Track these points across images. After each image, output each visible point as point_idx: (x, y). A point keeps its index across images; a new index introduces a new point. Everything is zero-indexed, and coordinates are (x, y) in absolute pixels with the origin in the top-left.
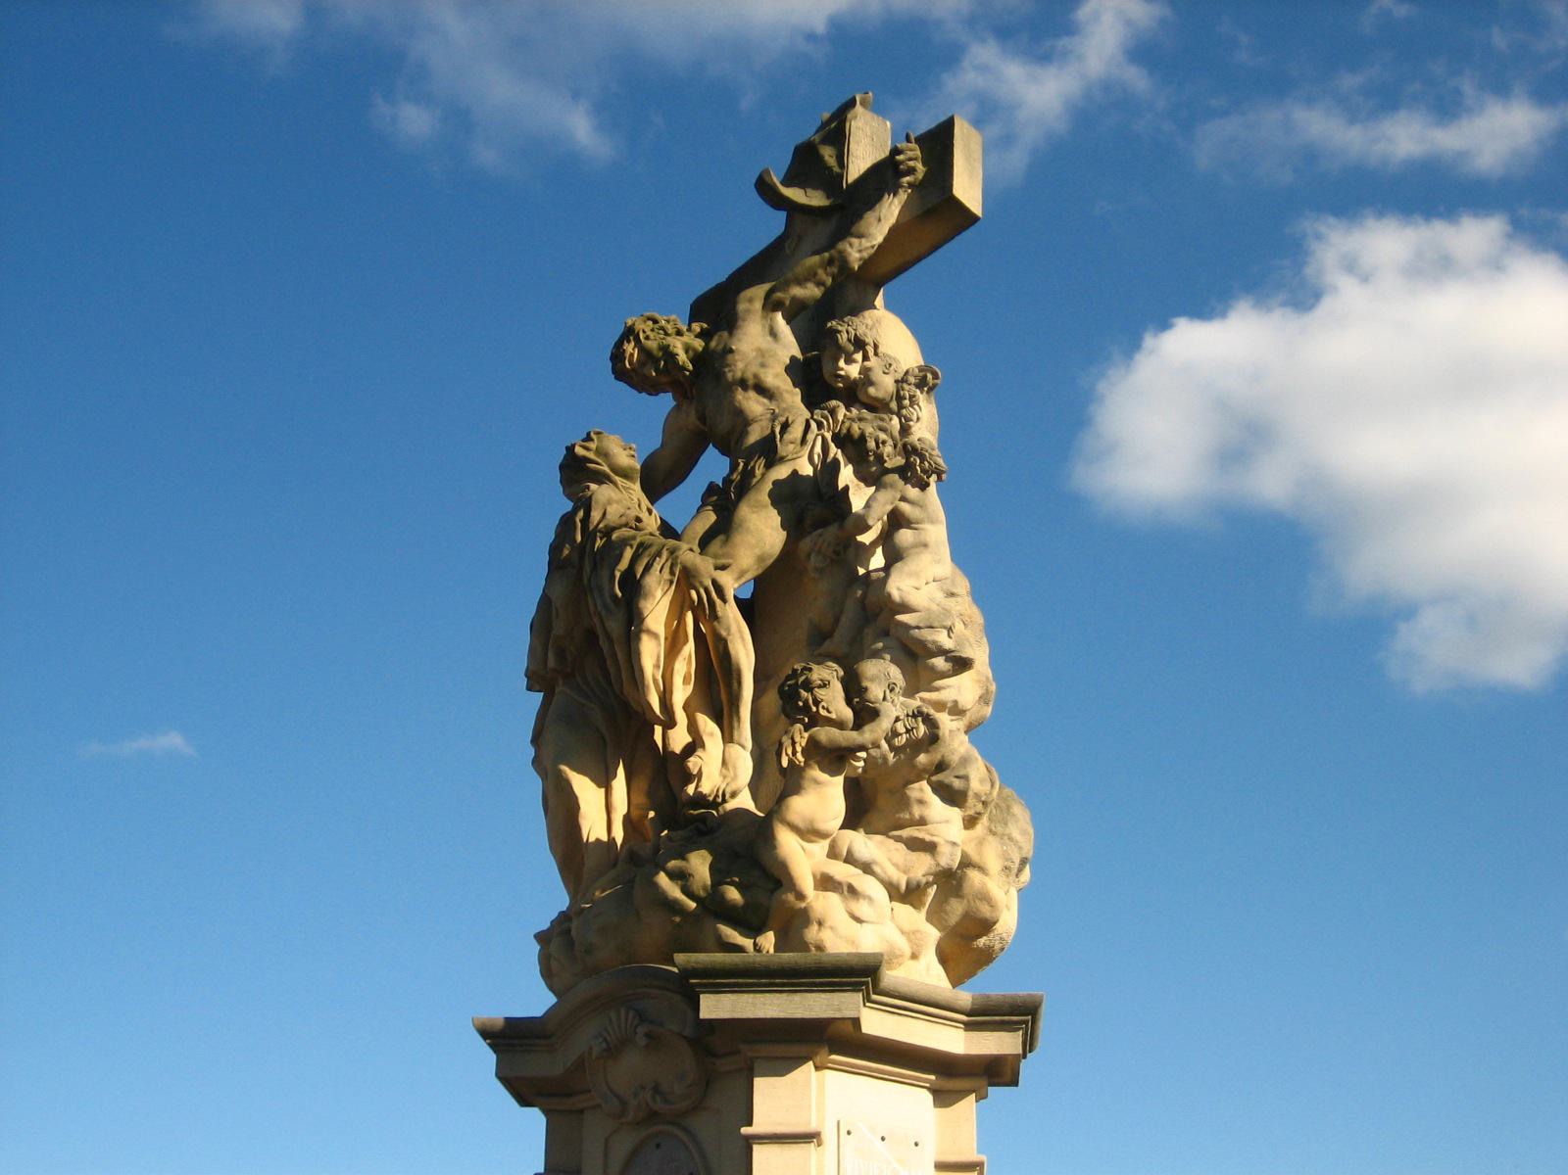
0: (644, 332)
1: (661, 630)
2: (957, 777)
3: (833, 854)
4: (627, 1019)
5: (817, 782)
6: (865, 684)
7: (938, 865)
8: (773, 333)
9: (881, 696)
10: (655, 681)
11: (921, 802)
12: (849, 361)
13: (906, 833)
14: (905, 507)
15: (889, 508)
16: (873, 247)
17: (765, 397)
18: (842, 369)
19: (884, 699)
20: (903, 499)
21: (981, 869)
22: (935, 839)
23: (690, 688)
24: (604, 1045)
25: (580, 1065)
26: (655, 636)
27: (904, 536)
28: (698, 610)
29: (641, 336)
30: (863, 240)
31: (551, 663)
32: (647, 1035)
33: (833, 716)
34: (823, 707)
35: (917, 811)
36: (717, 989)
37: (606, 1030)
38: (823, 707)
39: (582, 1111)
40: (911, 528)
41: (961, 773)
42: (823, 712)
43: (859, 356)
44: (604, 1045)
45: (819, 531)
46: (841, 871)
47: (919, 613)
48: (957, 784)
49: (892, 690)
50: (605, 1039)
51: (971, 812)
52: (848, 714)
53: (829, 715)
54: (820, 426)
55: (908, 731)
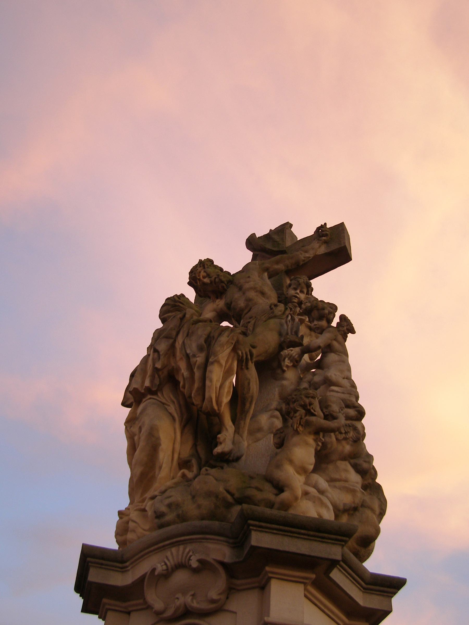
0: (207, 265)
1: (223, 362)
2: (365, 461)
3: (306, 483)
4: (183, 553)
5: (307, 444)
6: (330, 404)
7: (354, 502)
8: (262, 279)
9: (338, 411)
10: (216, 388)
11: (346, 471)
12: (302, 292)
13: (337, 484)
14: (335, 343)
15: (330, 341)
16: (309, 257)
17: (264, 297)
18: (298, 294)
19: (340, 412)
20: (335, 340)
21: (372, 510)
22: (355, 488)
23: (230, 398)
24: (165, 567)
25: (142, 580)
26: (221, 365)
27: (332, 357)
28: (240, 361)
29: (206, 266)
30: (306, 254)
31: (147, 383)
32: (200, 561)
33: (316, 413)
34: (312, 408)
35: (343, 475)
36: (261, 529)
37: (168, 560)
38: (312, 408)
39: (129, 613)
40: (336, 354)
41: (367, 460)
42: (312, 411)
43: (305, 291)
44: (165, 567)
45: (291, 349)
46: (312, 491)
47: (342, 388)
48: (365, 465)
49: (342, 410)
50: (166, 564)
51: (366, 482)
52: (322, 414)
53: (315, 413)
54: (291, 309)
55: (346, 433)
